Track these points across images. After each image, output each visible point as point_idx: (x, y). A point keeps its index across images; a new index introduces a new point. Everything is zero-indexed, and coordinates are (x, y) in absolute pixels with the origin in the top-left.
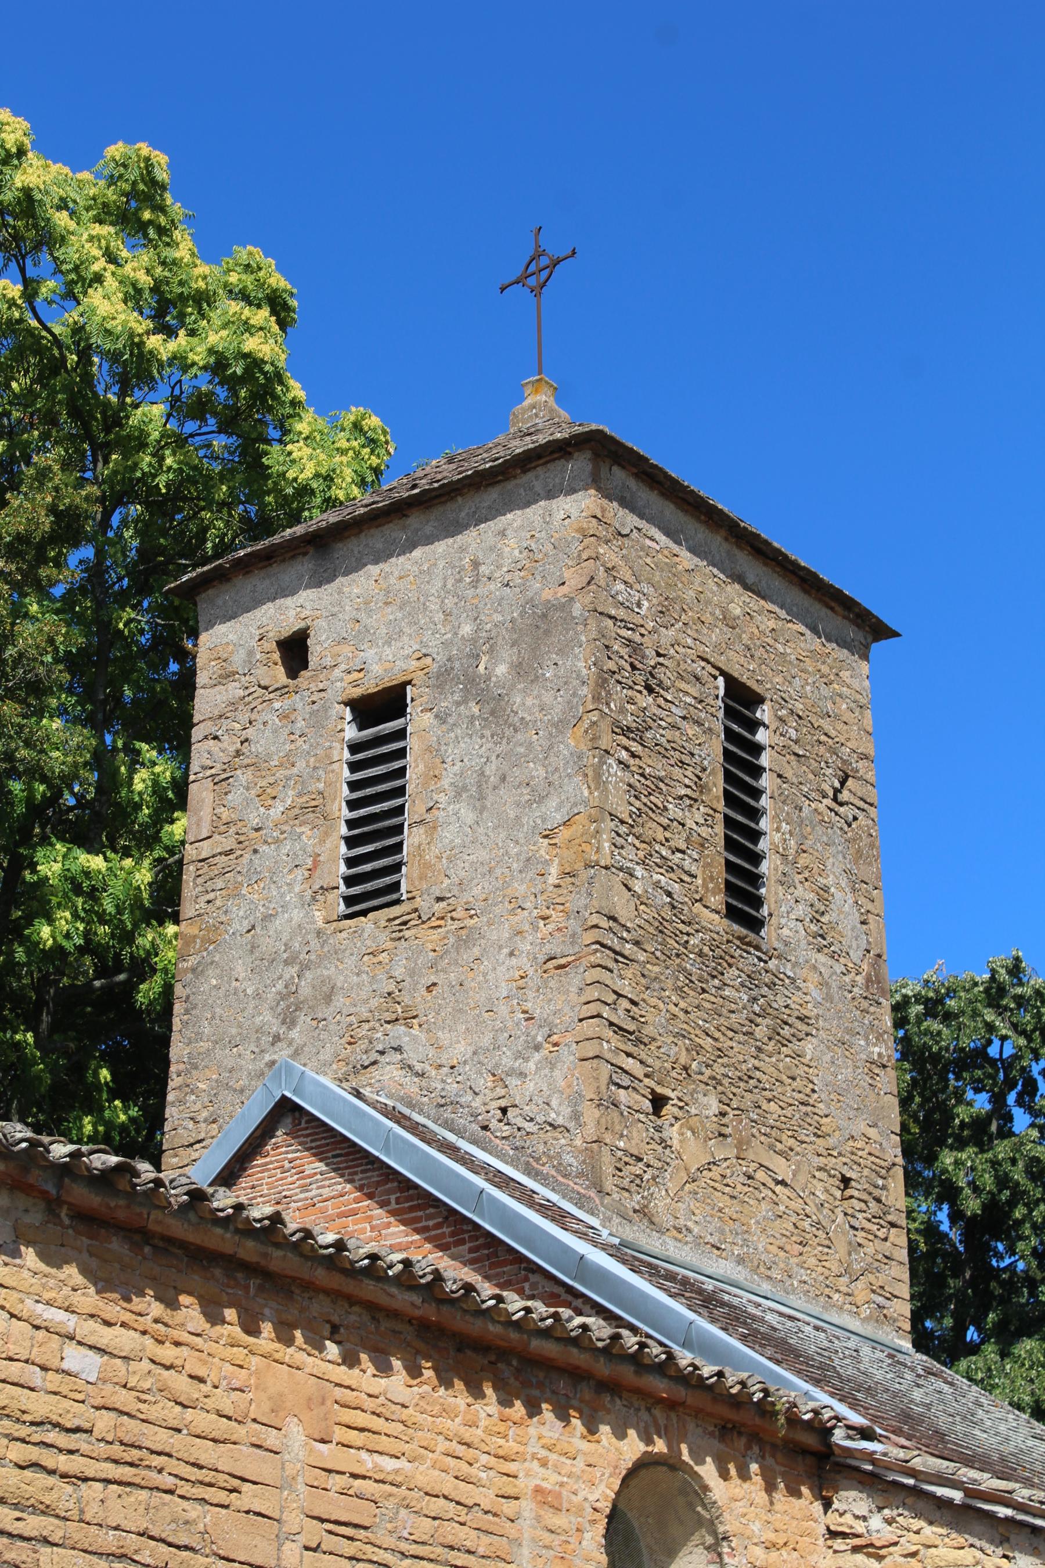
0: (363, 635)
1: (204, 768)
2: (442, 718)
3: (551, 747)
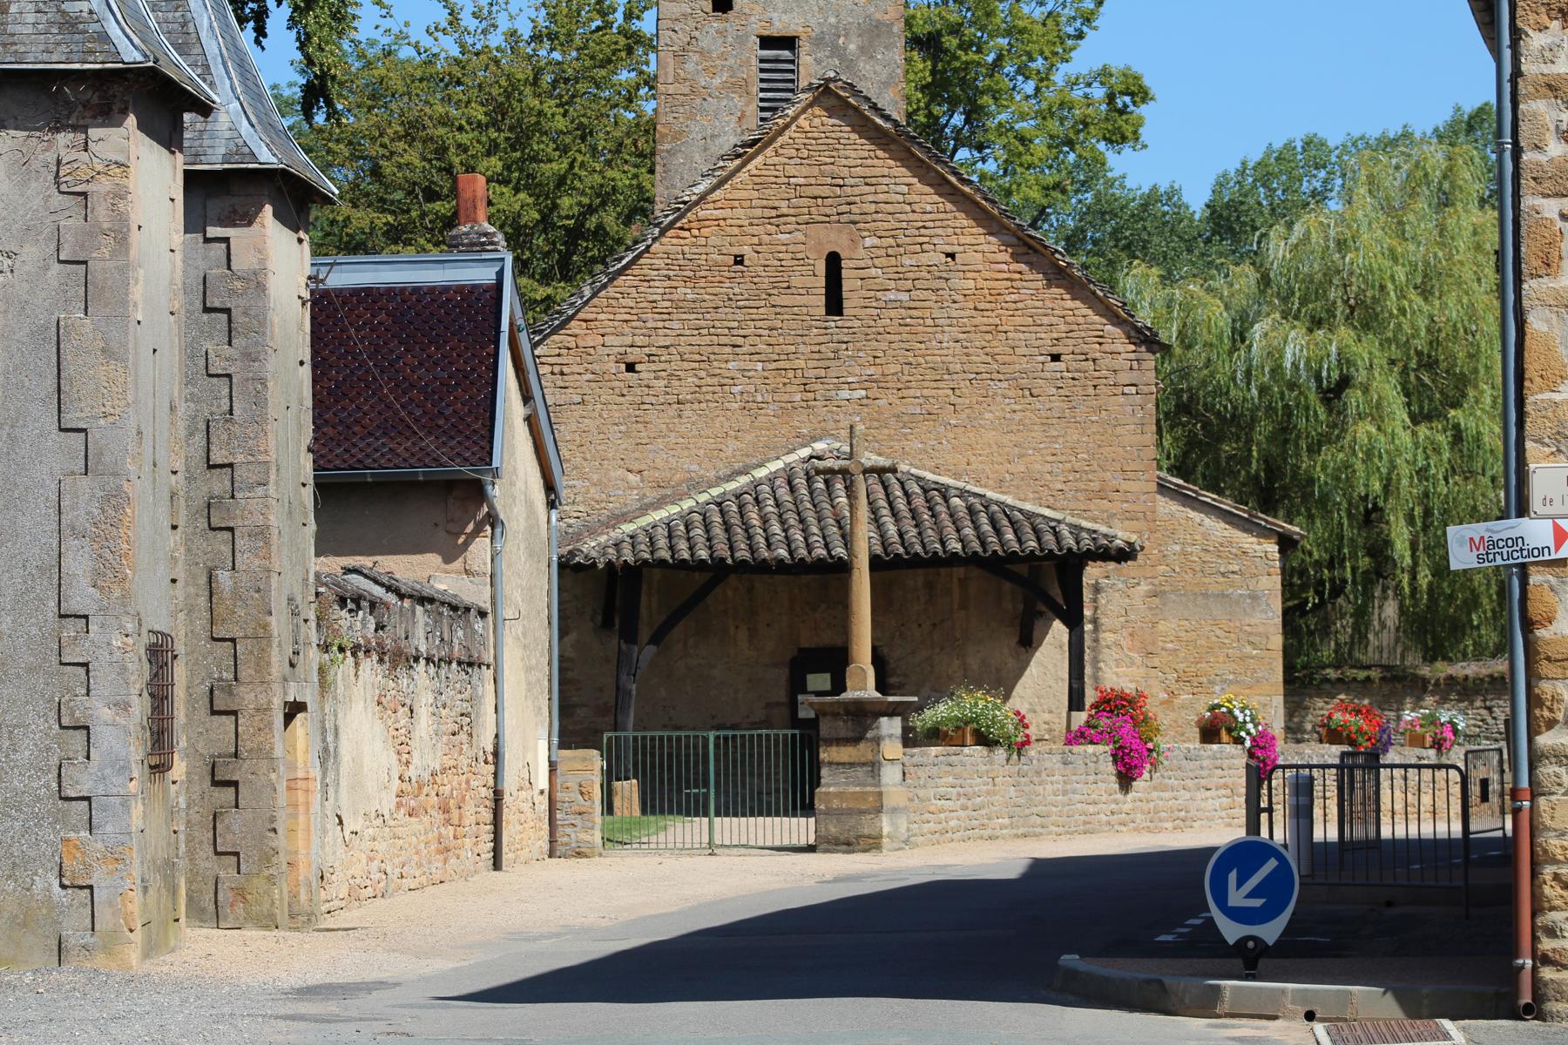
2: (818, 62)
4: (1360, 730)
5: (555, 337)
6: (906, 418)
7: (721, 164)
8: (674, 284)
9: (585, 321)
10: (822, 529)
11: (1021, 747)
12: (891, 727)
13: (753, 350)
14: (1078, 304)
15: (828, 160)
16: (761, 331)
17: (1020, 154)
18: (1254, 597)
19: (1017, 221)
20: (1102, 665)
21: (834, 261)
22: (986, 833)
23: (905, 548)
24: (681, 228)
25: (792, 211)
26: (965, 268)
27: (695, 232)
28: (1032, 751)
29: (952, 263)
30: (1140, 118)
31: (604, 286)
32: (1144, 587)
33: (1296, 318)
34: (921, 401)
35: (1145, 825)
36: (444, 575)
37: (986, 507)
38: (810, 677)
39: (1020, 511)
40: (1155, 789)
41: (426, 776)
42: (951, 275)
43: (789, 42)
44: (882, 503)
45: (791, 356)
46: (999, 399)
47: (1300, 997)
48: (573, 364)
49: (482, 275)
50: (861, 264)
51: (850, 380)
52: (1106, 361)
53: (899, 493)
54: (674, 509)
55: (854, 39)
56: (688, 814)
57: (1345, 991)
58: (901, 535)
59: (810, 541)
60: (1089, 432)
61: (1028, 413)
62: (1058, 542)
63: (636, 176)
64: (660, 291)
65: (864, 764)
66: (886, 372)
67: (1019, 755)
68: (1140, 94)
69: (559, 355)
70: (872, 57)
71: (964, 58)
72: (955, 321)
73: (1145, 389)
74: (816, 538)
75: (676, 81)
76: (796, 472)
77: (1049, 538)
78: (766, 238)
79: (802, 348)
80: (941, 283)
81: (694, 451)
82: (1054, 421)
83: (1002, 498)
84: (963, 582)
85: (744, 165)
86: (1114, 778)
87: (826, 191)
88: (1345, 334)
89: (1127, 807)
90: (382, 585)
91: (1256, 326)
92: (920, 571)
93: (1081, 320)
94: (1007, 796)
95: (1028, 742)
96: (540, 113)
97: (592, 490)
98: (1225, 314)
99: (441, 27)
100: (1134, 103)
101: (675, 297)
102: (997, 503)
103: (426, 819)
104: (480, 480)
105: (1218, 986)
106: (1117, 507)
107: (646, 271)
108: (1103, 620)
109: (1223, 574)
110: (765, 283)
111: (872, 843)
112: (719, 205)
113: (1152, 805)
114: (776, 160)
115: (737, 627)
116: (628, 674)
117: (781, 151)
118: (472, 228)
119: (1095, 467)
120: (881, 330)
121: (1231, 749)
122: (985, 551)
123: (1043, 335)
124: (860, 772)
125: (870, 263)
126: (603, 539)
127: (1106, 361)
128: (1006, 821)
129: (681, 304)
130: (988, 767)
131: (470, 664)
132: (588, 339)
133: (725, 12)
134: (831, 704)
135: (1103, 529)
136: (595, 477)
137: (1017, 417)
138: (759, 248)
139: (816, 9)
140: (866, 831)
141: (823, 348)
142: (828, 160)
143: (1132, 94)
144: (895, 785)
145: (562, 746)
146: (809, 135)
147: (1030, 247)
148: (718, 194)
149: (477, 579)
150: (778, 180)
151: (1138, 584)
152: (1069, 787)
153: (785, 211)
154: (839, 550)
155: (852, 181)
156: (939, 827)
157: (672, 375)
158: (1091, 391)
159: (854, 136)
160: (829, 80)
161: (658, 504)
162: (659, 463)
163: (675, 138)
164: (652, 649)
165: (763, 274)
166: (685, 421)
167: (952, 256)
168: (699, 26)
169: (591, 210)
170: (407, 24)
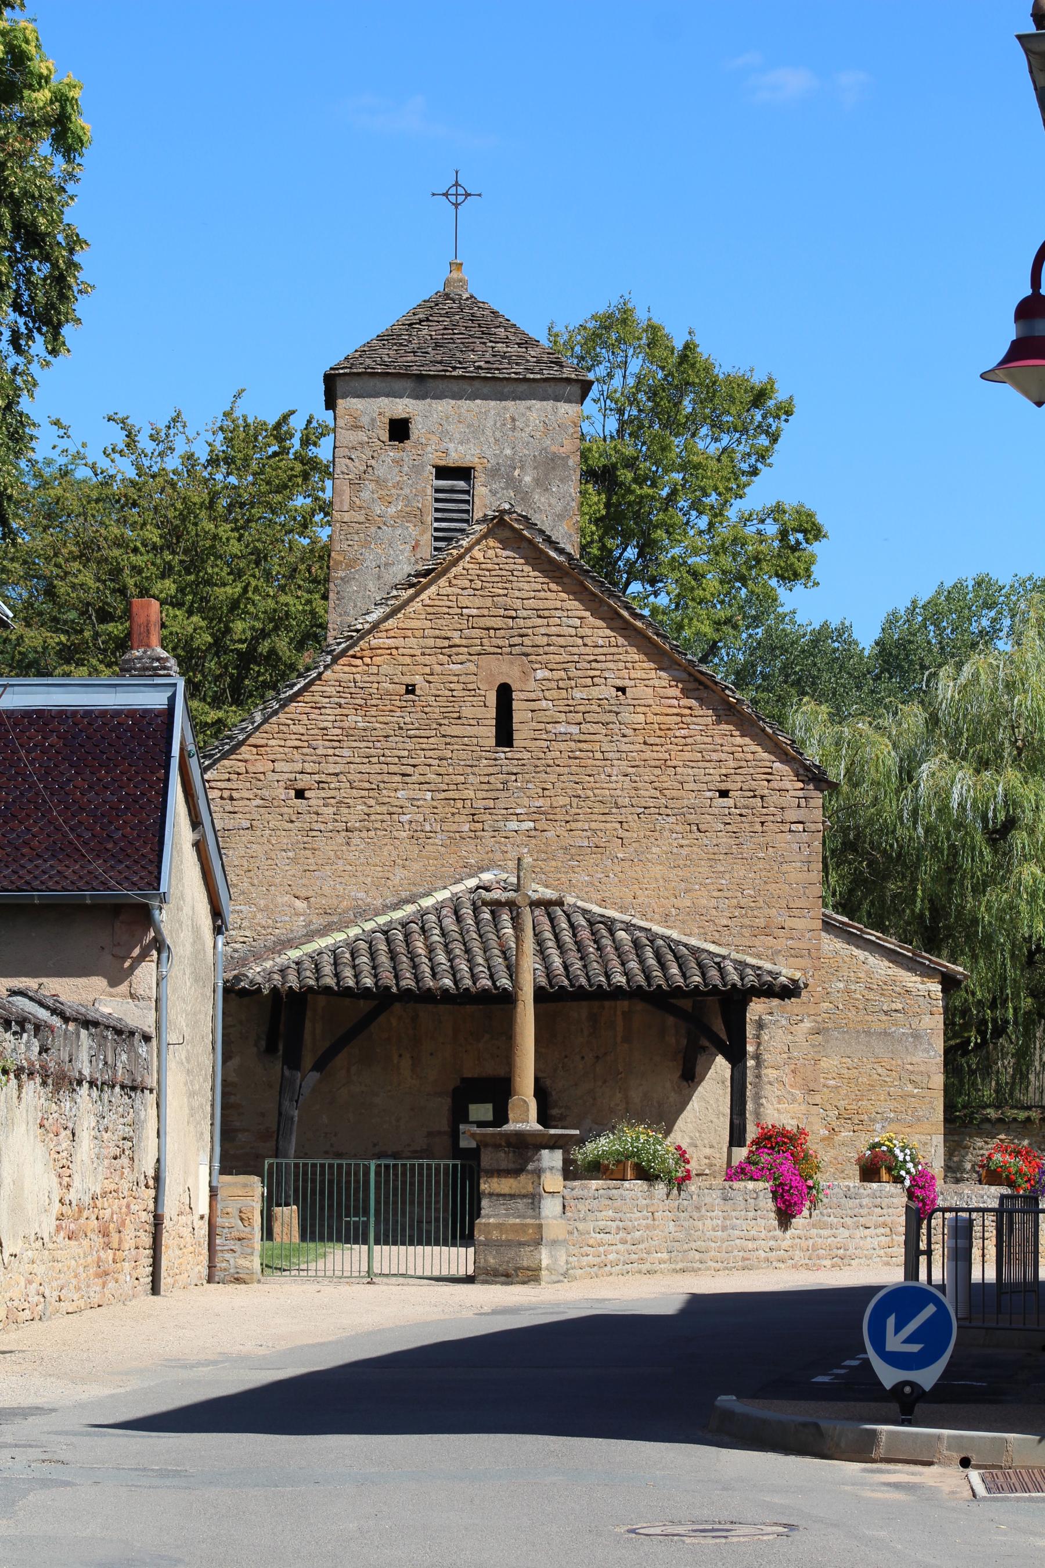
0: (444, 435)
1: (343, 473)
2: (494, 493)
3: (554, 526)
4: (1020, 1171)
5: (225, 762)
6: (573, 851)
7: (395, 593)
8: (345, 711)
9: (256, 746)
10: (487, 960)
11: (679, 1182)
12: (552, 1159)
13: (422, 779)
14: (747, 740)
15: (501, 592)
16: (430, 761)
17: (692, 589)
18: (916, 1036)
19: (689, 657)
20: (763, 1101)
21: (505, 693)
22: (645, 1267)
23: (569, 980)
24: (354, 657)
25: (464, 642)
26: (636, 702)
27: (368, 660)
28: (692, 1187)
29: (622, 697)
30: (813, 556)
31: (275, 713)
32: (807, 1024)
33: (963, 758)
34: (589, 834)
35: (803, 1262)
36: (109, 999)
37: (651, 941)
38: (472, 1107)
39: (685, 945)
40: (814, 1226)
41: (87, 1200)
42: (622, 709)
43: (464, 473)
44: (548, 935)
45: (460, 787)
46: (666, 834)
47: (955, 1444)
48: (242, 789)
49: (154, 699)
50: (533, 696)
51: (518, 811)
52: (774, 799)
53: (564, 925)
54: (340, 937)
55: (529, 471)
56: (347, 1242)
57: (1000, 1439)
58: (566, 967)
59: (475, 971)
60: (755, 868)
61: (695, 848)
62: (723, 977)
63: (309, 602)
64: (333, 718)
65: (524, 1196)
66: (555, 804)
67: (679, 1190)
68: (813, 531)
69: (229, 780)
70: (547, 490)
71: (639, 492)
72: (624, 755)
73: (813, 827)
74: (481, 968)
75: (352, 507)
76: (462, 902)
77: (713, 973)
78: (438, 668)
79: (471, 779)
80: (612, 717)
81: (361, 879)
82: (721, 857)
83: (668, 932)
84: (627, 1016)
85: (417, 594)
86: (773, 1215)
87: (498, 622)
88: (1012, 775)
89: (785, 1244)
90: (46, 1007)
91: (924, 766)
92: (584, 1003)
93: (750, 757)
94: (667, 1230)
95: (688, 1177)
96: (215, 537)
97: (259, 916)
98: (893, 753)
99: (118, 449)
100: (807, 541)
101: (346, 724)
102: (663, 937)
103: (85, 1243)
104: (147, 904)
105: (875, 1431)
106: (782, 943)
107: (317, 698)
108: (766, 1056)
109: (886, 1013)
110: (436, 713)
111: (531, 1276)
112: (391, 634)
113: (810, 1242)
114: (450, 590)
115: (400, 1056)
116: (291, 1100)
117: (454, 582)
118: (145, 652)
119: (762, 904)
120: (551, 762)
121: (890, 1188)
122: (649, 985)
123: (712, 771)
124: (520, 1204)
125: (541, 694)
126: (268, 964)
127: (774, 799)
128: (665, 1256)
129: (351, 732)
130: (648, 1201)
131: (134, 1089)
132: (258, 764)
133: (401, 441)
134: (493, 1135)
135: (768, 966)
136: (262, 903)
137: (684, 852)
138: (430, 678)
139: (492, 440)
140: (525, 1264)
141: (492, 779)
142: (501, 592)
143: (805, 532)
144: (555, 1218)
145: (223, 1172)
146: (483, 566)
147: (701, 683)
148: (391, 623)
149: (142, 1004)
150: (451, 611)
151: (802, 1021)
152: (728, 1222)
153: (457, 641)
154: (504, 981)
155: (525, 613)
156: (597, 1260)
157: (341, 802)
158: (758, 827)
159: (527, 568)
160: (503, 512)
161: (324, 931)
162: (326, 890)
163: (349, 566)
164: (315, 1076)
165: (435, 704)
166: (354, 848)
167: (622, 690)
168: (375, 455)
169: (264, 634)
170: (84, 445)
